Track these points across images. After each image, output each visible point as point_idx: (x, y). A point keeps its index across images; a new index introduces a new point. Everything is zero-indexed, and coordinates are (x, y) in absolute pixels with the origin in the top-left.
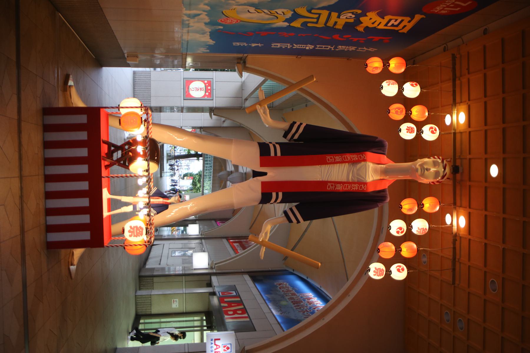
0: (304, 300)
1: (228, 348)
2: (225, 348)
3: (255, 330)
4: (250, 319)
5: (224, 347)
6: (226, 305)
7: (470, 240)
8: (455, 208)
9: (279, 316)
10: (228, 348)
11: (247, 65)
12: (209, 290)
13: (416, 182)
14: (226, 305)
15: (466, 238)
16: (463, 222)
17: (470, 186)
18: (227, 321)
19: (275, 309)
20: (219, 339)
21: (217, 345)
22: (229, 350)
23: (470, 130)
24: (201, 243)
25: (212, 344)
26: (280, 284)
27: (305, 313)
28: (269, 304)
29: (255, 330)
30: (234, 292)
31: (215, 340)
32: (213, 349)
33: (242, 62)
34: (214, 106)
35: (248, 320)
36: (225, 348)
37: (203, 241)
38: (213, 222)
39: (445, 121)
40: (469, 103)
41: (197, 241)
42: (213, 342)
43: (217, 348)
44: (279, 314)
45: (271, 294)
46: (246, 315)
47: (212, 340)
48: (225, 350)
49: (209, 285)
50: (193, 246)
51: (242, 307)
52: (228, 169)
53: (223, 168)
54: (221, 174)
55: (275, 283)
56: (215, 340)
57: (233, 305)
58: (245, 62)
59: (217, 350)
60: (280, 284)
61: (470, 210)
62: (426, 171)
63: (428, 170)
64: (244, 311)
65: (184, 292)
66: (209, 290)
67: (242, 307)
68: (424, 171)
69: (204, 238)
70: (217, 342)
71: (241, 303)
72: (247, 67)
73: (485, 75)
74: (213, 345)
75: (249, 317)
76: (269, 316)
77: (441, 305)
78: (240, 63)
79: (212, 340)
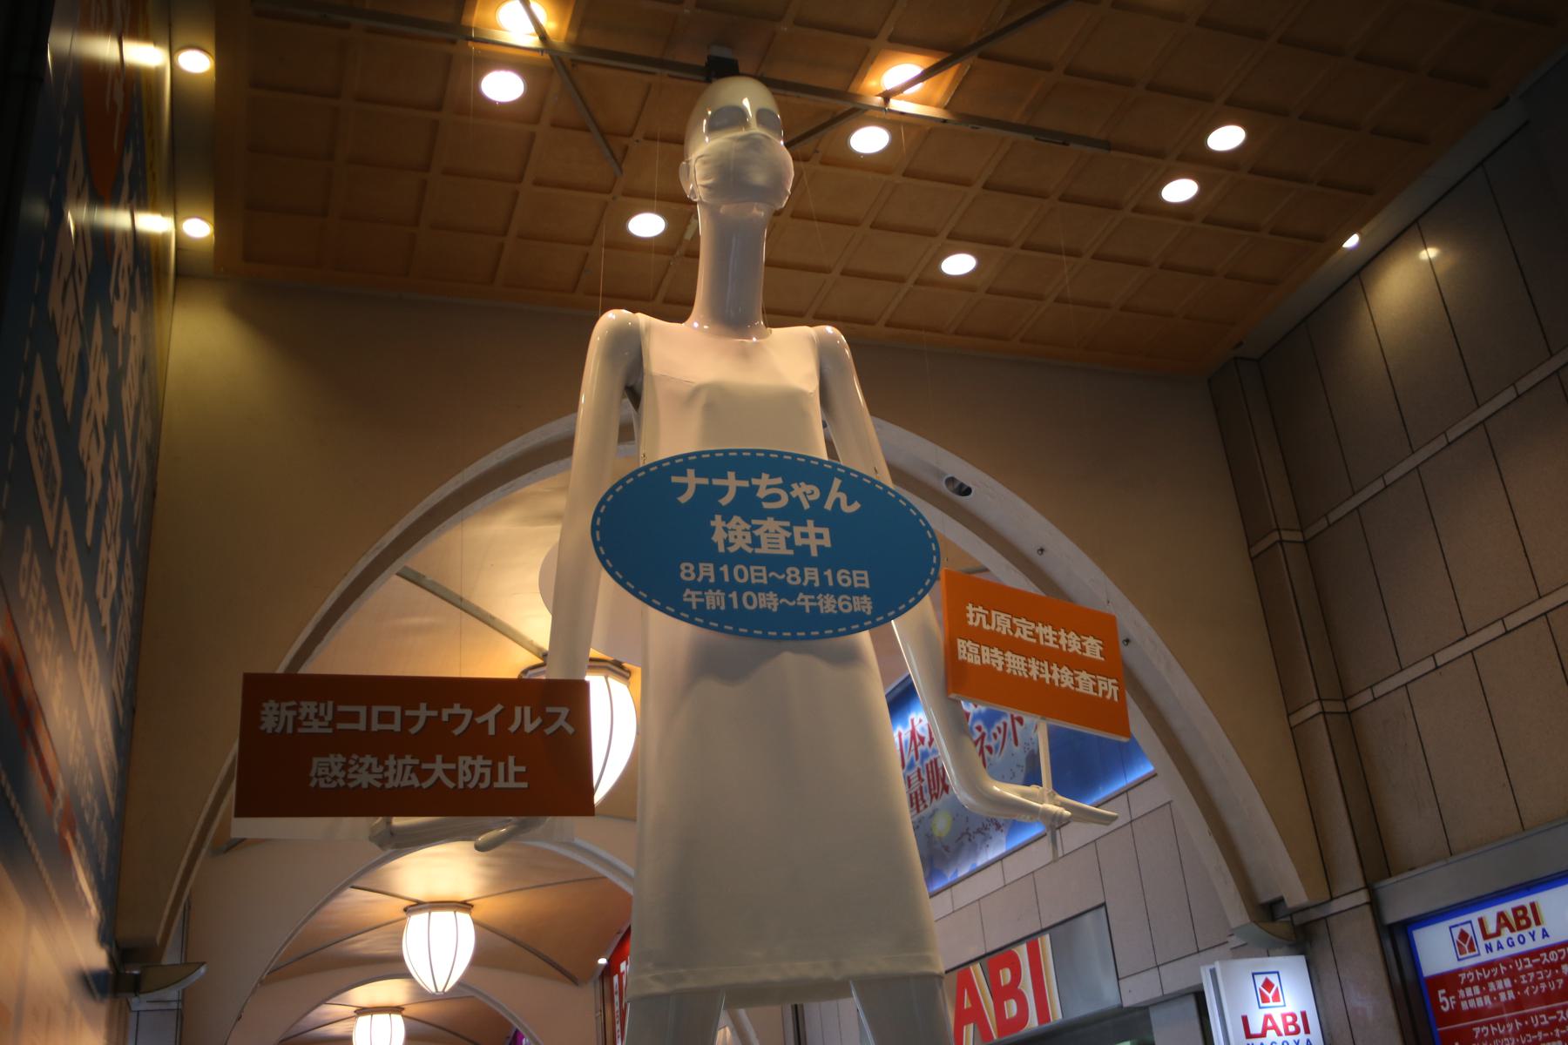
0: (925, 755)
1: (1268, 985)
2: (1270, 996)
3: (1104, 905)
4: (1042, 931)
5: (1265, 999)
17: (798, 22)
18: (1057, 1015)
19: (975, 851)
20: (1245, 1020)
21: (1265, 1029)
22: (1273, 979)
27: (993, 743)
28: (950, 878)
29: (1104, 905)
31: (1249, 1035)
35: (1045, 942)
43: (1275, 1027)
44: (1003, 837)
46: (1022, 952)
48: (1276, 998)
51: (977, 971)
57: (967, 1004)
67: (977, 971)
70: (1256, 1028)
75: (1031, 940)
76: (1018, 867)
77: (1135, 210)
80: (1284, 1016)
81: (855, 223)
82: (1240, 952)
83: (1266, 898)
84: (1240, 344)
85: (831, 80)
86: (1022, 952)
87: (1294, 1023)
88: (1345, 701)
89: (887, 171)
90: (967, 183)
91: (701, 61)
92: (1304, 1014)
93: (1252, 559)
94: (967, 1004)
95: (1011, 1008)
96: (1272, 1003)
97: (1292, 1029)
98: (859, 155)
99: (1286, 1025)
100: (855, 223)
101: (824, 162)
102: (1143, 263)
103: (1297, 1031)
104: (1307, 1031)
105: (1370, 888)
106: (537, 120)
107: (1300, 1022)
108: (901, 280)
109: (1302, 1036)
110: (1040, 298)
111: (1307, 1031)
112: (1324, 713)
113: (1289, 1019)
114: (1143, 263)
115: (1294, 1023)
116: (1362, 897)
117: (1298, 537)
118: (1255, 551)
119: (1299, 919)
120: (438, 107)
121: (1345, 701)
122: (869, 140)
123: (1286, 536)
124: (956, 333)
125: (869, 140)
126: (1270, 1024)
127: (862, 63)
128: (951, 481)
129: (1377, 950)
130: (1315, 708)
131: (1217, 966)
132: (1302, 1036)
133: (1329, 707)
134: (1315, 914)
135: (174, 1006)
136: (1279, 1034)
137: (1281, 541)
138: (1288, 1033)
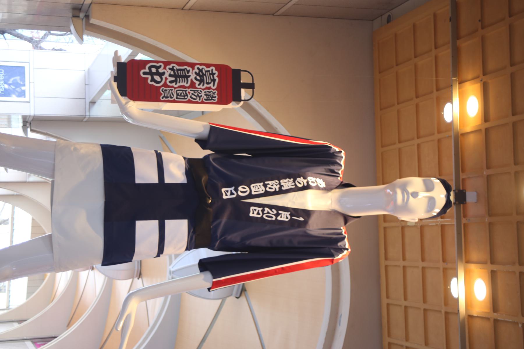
7: (496, 321)
11: (92, 21)
13: (397, 217)
15: (488, 319)
16: (481, 290)
23: (487, 125)
33: (82, 15)
39: (443, 115)
40: (485, 78)
58: (87, 17)
61: (495, 267)
63: (415, 195)
72: (93, 25)
73: (511, 28)
78: (78, 17)
81: (425, 301)
85: (474, 255)
89: (446, 304)
100: (425, 301)
101: (445, 270)
106: (439, 132)
120: (437, 90)
135: (87, 114)
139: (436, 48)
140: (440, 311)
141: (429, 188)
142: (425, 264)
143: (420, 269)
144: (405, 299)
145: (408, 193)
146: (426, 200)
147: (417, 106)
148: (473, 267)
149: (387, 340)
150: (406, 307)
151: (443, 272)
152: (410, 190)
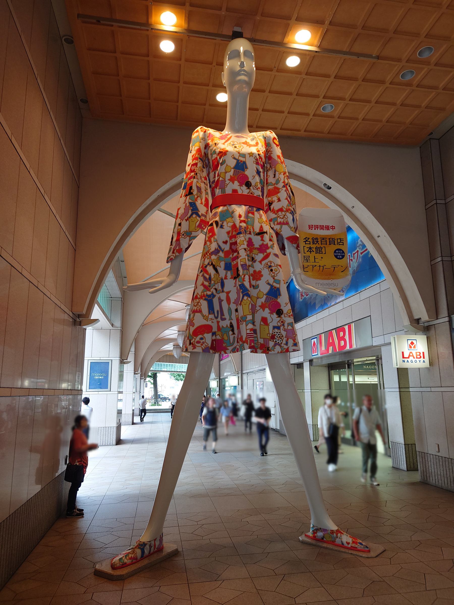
1: (412, 343)
2: (413, 346)
6: (331, 348)
7: (331, 23)
8: (286, 44)
9: (347, 293)
10: (412, 343)
12: (306, 366)
14: (331, 348)
18: (354, 347)
20: (403, 353)
21: (409, 356)
22: (414, 342)
24: (247, 373)
25: (408, 361)
26: (302, 295)
30: (313, 341)
32: (414, 360)
34: (118, 358)
35: (353, 325)
36: (413, 346)
37: (244, 372)
38: (221, 362)
41: (245, 377)
42: (406, 360)
43: (413, 356)
45: (315, 304)
46: (346, 328)
47: (404, 361)
48: (414, 347)
49: (300, 366)
50: (250, 382)
51: (334, 332)
52: (172, 349)
53: (168, 353)
54: (176, 356)
55: (301, 300)
56: (403, 357)
57: (331, 341)
59: (415, 357)
60: (302, 295)
62: (244, 68)
64: (340, 329)
65: (310, 391)
66: (306, 366)
67: (334, 332)
68: (244, 71)
69: (242, 371)
70: (406, 355)
71: (329, 333)
74: (409, 360)
79: (404, 361)
80: (416, 353)
81: (290, 94)
82: (407, 333)
83: (416, 317)
84: (432, 133)
85: (277, 38)
86: (346, 328)
87: (419, 355)
88: (451, 257)
90: (328, 76)
91: (231, 34)
92: (423, 353)
93: (426, 210)
94: (331, 341)
95: (342, 343)
96: (413, 349)
97: (419, 357)
98: (290, 67)
99: (417, 355)
100: (290, 94)
101: (278, 71)
102: (394, 104)
103: (420, 357)
104: (424, 358)
105: (449, 316)
106: (180, 60)
107: (422, 355)
108: (308, 114)
109: (422, 359)
110: (357, 119)
111: (424, 358)
112: (442, 261)
113: (418, 354)
114: (394, 104)
115: (419, 355)
116: (447, 319)
117: (443, 202)
118: (427, 207)
119: (426, 324)
120: (148, 56)
121: (451, 257)
122: (293, 62)
123: (439, 201)
124: (328, 133)
125: (293, 62)
126: (411, 354)
127: (286, 30)
128: (325, 184)
129: (449, 335)
130: (439, 259)
131: (396, 336)
132: (422, 359)
133: (445, 259)
134: (431, 323)
136: (414, 358)
137: (436, 203)
138: (417, 358)
139: (115, 52)
140: (304, 79)
141: (236, 54)
142: (268, 91)
143: (269, 94)
144: (283, 112)
145: (240, 71)
146: (246, 58)
147: (155, 80)
148: (286, 40)
149: (302, 133)
150: (289, 113)
151: (279, 72)
152: (238, 68)
